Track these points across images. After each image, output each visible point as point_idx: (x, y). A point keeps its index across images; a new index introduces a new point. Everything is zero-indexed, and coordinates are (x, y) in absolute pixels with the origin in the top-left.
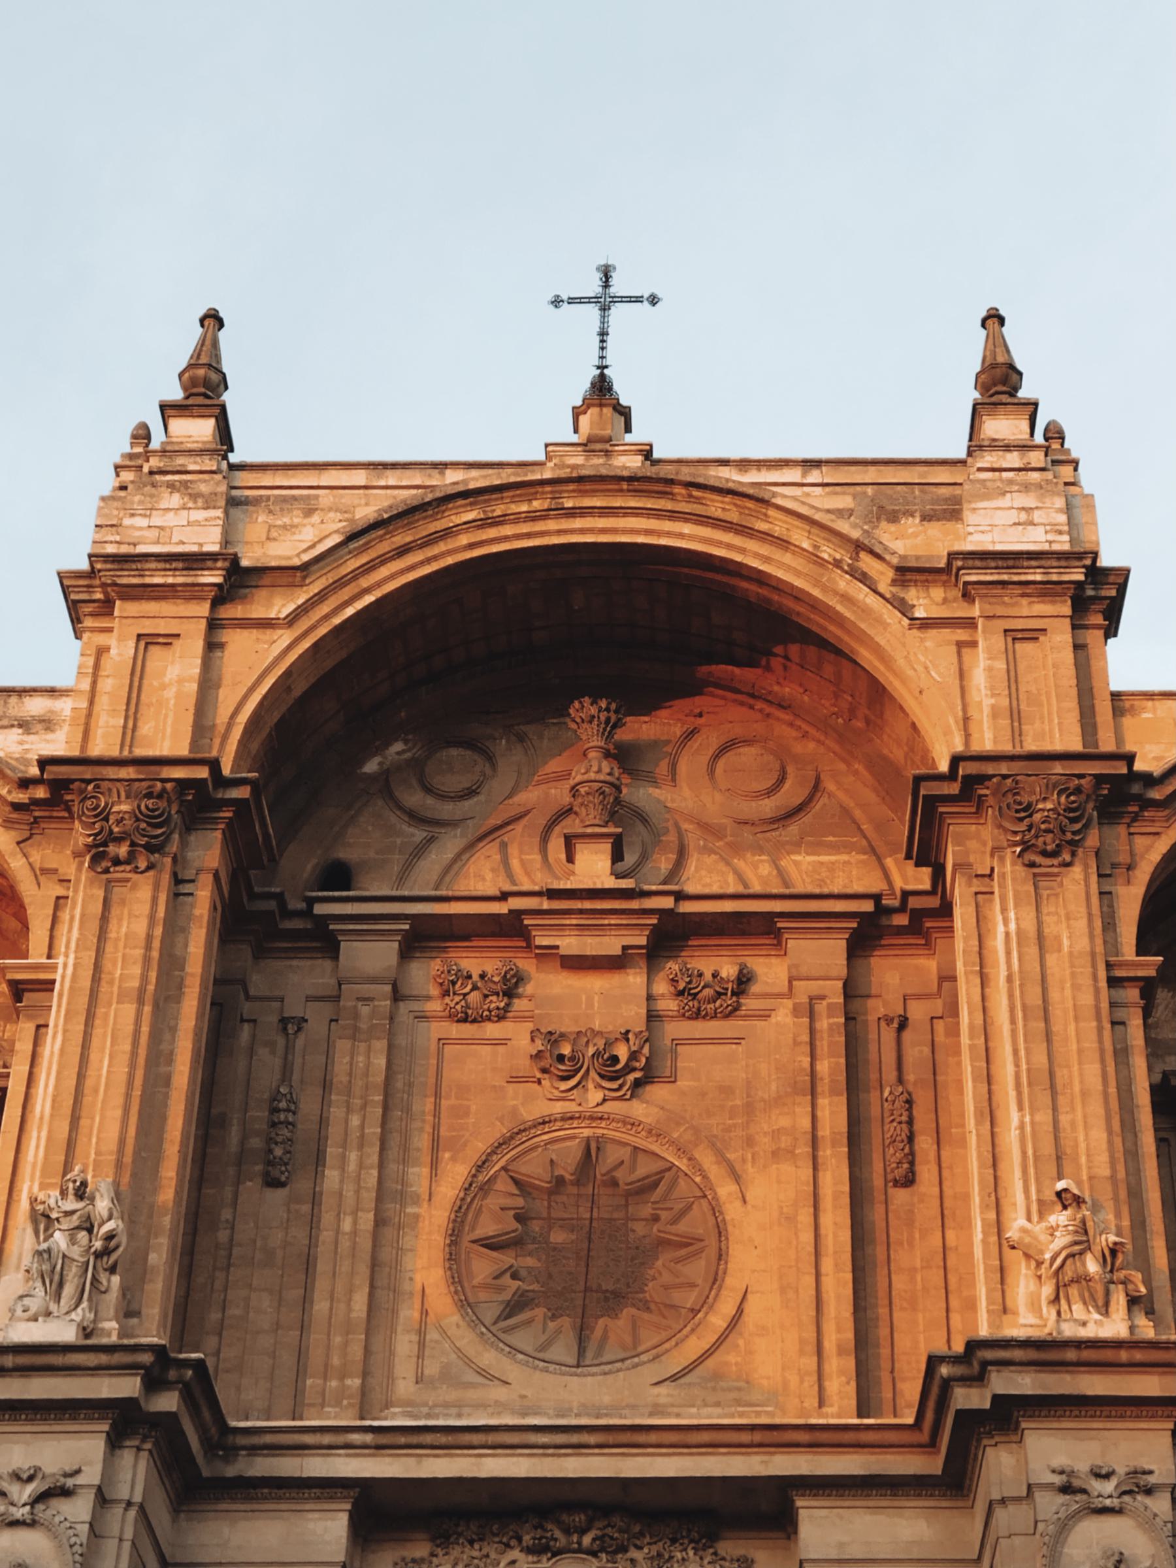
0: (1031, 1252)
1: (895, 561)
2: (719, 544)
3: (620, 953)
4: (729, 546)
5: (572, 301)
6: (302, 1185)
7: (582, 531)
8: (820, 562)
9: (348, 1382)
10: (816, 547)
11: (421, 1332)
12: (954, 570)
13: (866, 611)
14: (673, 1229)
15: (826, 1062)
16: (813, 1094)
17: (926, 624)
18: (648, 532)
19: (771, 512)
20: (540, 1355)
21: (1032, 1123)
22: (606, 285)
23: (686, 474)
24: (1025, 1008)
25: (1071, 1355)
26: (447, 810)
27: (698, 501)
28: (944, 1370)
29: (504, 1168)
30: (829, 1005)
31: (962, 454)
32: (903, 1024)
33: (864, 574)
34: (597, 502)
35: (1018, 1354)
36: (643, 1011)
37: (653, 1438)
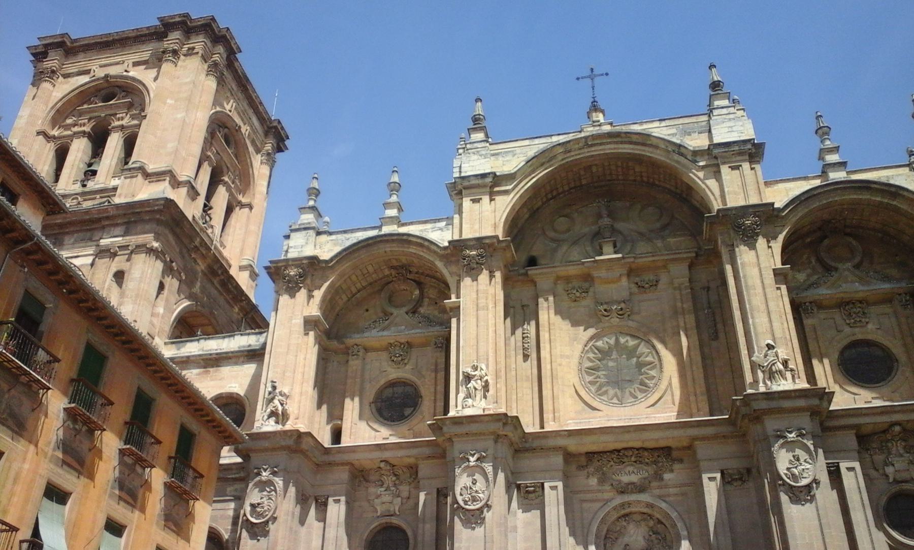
0: (760, 364)
1: (691, 148)
2: (637, 150)
4: (640, 150)
5: (582, 78)
7: (595, 151)
8: (668, 152)
10: (667, 147)
13: (684, 166)
18: (615, 149)
19: (652, 138)
20: (611, 401)
22: (592, 70)
23: (625, 129)
25: (776, 395)
28: (738, 403)
29: (593, 345)
30: (686, 287)
32: (708, 289)
33: (682, 153)
34: (599, 142)
36: (628, 293)
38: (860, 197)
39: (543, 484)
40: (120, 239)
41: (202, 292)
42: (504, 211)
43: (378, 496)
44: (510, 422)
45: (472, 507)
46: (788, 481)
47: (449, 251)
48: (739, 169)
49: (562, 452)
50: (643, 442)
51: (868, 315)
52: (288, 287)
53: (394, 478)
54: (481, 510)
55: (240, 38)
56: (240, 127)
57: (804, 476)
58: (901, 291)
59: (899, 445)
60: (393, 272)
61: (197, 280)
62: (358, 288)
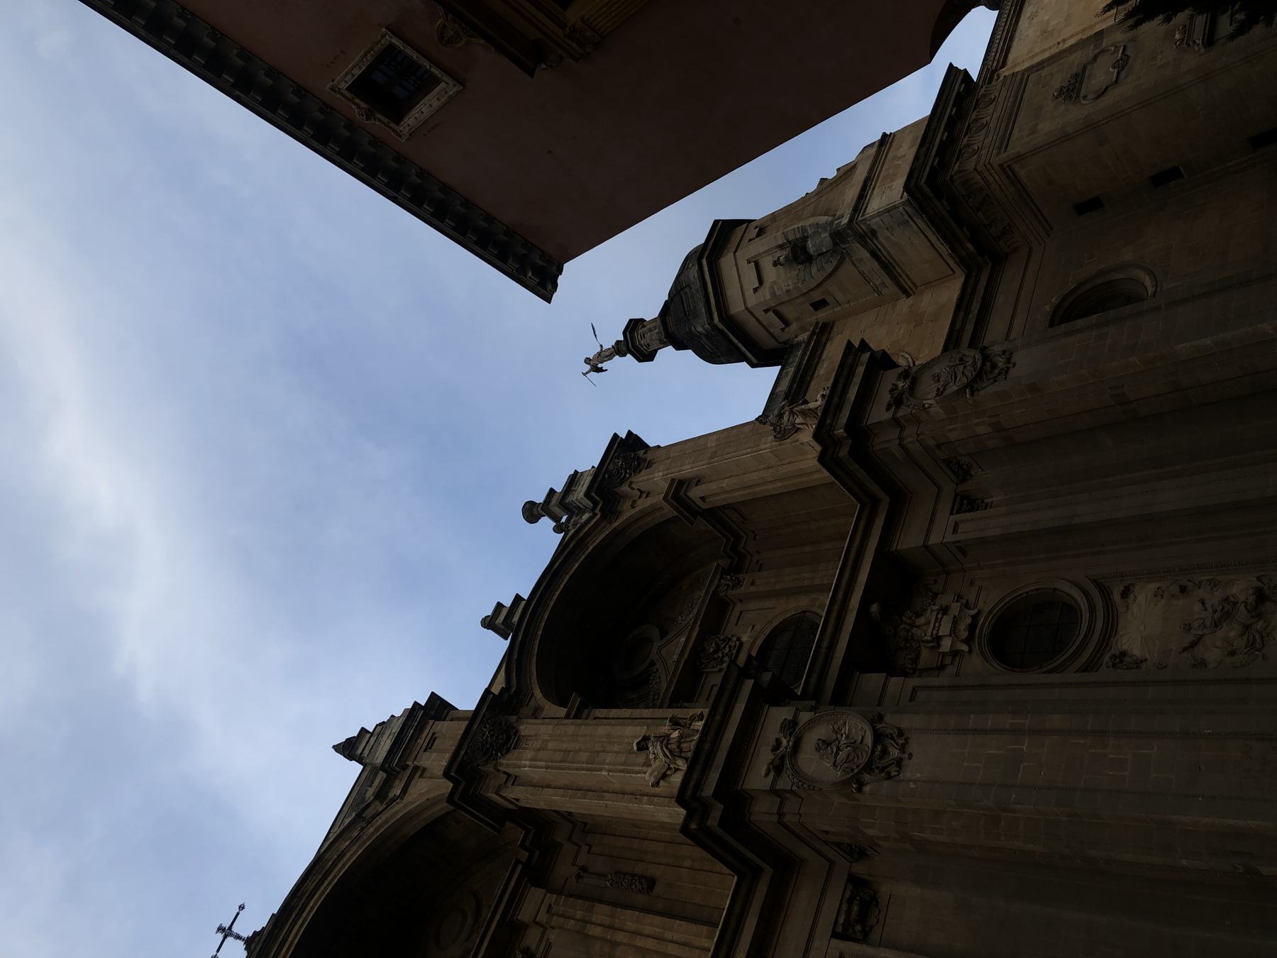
0: (663, 771)
5: (218, 951)
12: (389, 770)
13: (387, 821)
15: (578, 912)
16: (587, 922)
17: (405, 791)
19: (327, 856)
21: (608, 764)
24: (561, 761)
25: (707, 746)
27: (304, 893)
28: (693, 826)
30: (554, 904)
31: (362, 767)
32: (584, 869)
33: (372, 817)
35: (695, 776)
38: (562, 586)
46: (856, 771)
48: (435, 738)
51: (730, 636)
57: (859, 741)
58: (716, 582)
59: (909, 621)
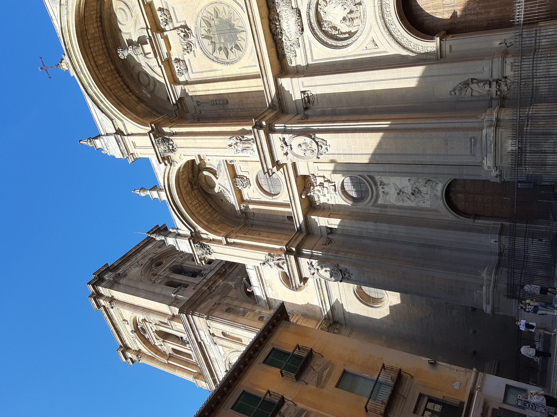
3: (163, 39)
6: (226, 97)
9: (259, 81)
11: (246, 67)
14: (214, 15)
26: (151, 80)
37: (250, 14)
39: (301, 92)
40: (205, 333)
41: (234, 281)
42: (136, 126)
43: (325, 195)
44: (258, 124)
45: (316, 148)
47: (166, 162)
49: (280, 79)
50: (263, 18)
52: (209, 254)
53: (312, 188)
54: (317, 143)
55: (99, 266)
56: (151, 258)
60: (195, 187)
61: (228, 284)
62: (209, 207)
